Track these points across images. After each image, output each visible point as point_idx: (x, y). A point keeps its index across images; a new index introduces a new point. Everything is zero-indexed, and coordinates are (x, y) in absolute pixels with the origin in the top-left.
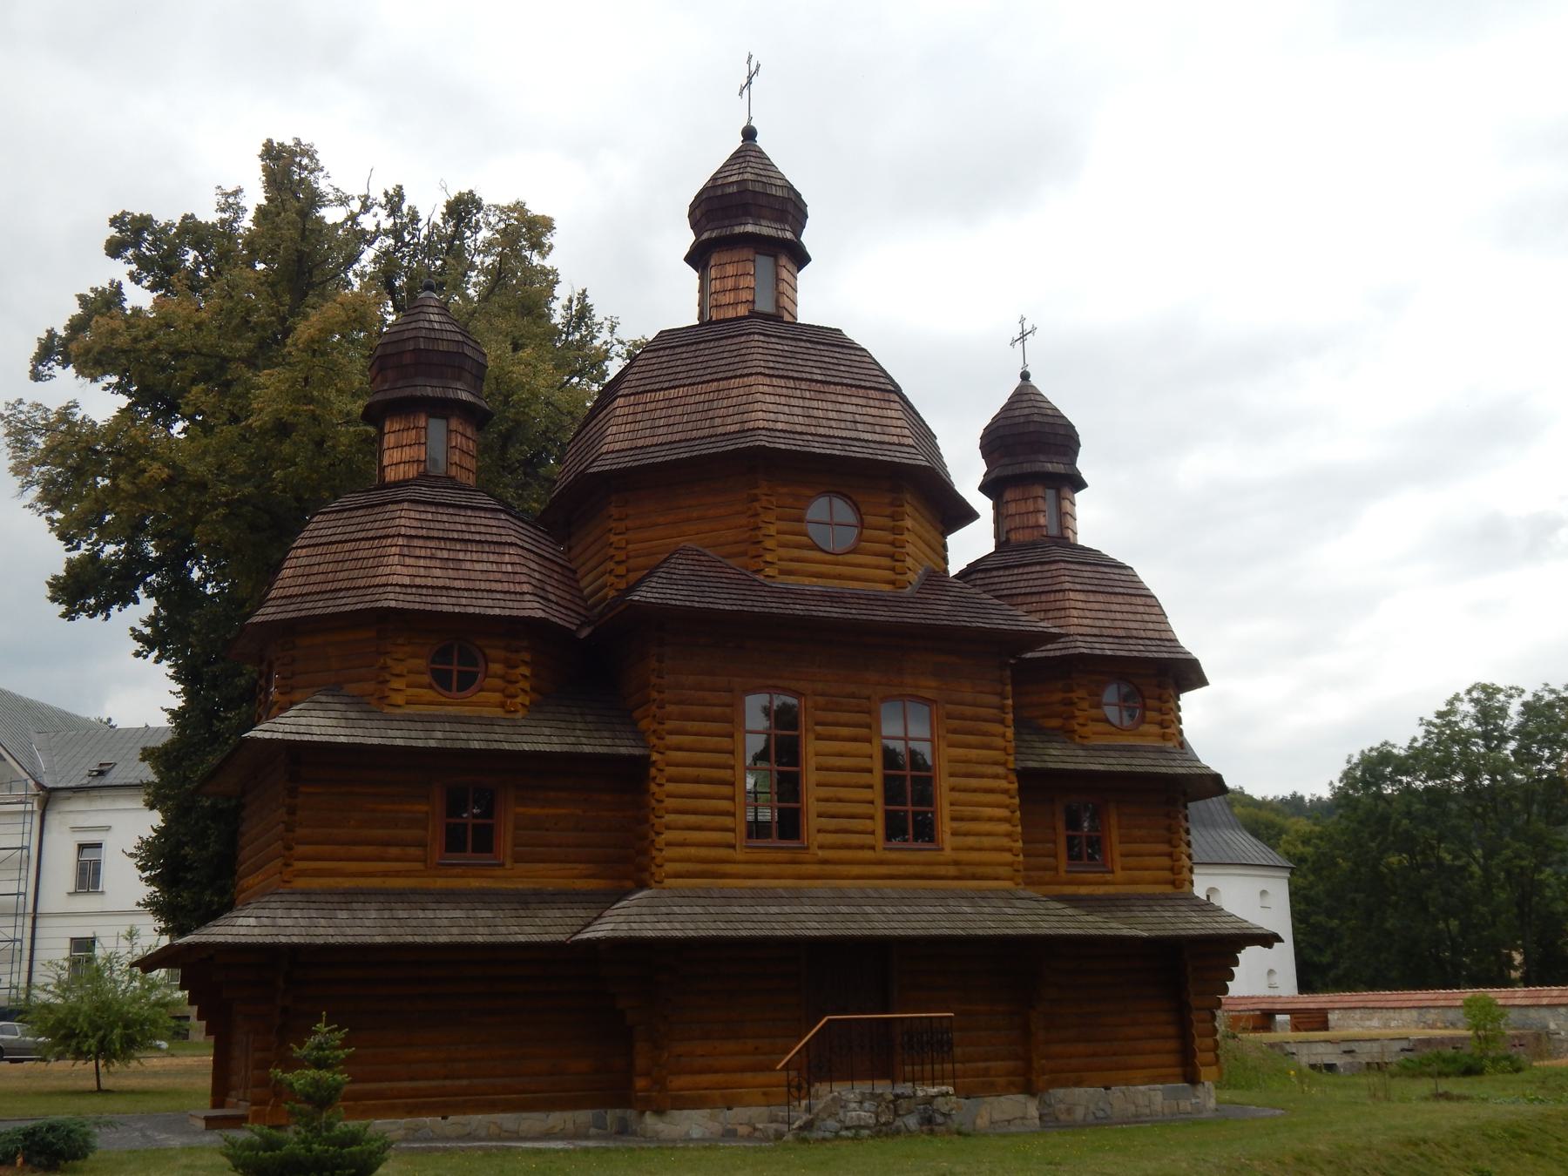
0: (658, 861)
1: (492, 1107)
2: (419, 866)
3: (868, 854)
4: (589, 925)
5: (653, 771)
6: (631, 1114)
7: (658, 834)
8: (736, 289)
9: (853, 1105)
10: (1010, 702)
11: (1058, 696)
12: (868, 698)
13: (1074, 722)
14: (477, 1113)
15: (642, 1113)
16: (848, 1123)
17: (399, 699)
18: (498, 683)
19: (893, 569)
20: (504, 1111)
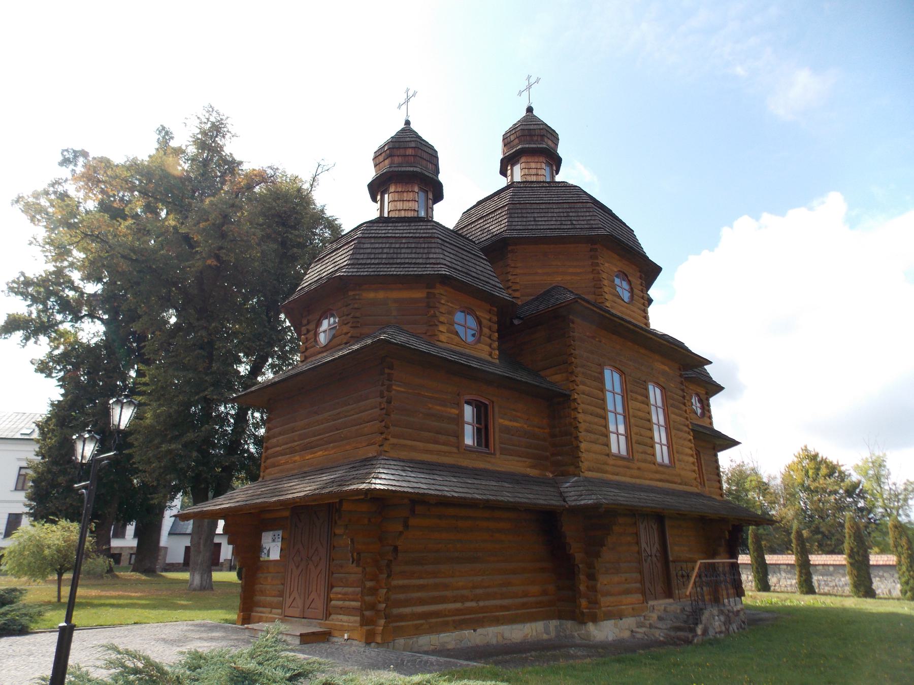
1: (498, 621)
2: (455, 450)
5: (574, 405)
6: (569, 624)
8: (537, 175)
14: (490, 626)
17: (443, 338)
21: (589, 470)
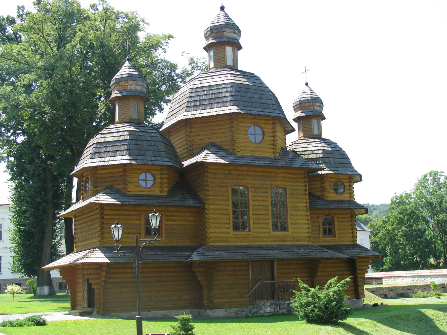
0: (208, 237)
3: (267, 235)
4: (190, 256)
6: (202, 310)
7: (208, 229)
9: (268, 307)
10: (307, 188)
11: (319, 186)
12: (267, 188)
13: (325, 193)
14: (158, 310)
15: (206, 310)
16: (267, 311)
18: (159, 185)
19: (273, 148)
20: (165, 310)
21: (213, 242)
